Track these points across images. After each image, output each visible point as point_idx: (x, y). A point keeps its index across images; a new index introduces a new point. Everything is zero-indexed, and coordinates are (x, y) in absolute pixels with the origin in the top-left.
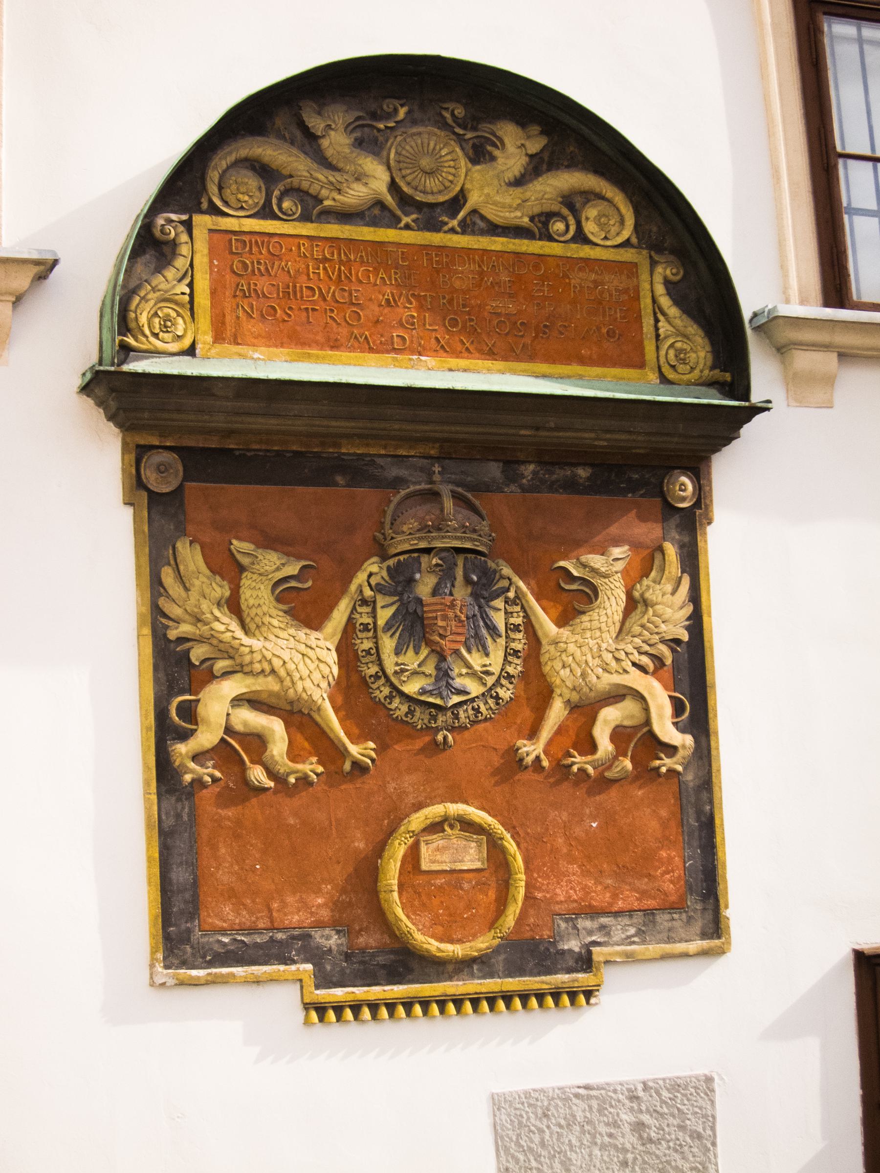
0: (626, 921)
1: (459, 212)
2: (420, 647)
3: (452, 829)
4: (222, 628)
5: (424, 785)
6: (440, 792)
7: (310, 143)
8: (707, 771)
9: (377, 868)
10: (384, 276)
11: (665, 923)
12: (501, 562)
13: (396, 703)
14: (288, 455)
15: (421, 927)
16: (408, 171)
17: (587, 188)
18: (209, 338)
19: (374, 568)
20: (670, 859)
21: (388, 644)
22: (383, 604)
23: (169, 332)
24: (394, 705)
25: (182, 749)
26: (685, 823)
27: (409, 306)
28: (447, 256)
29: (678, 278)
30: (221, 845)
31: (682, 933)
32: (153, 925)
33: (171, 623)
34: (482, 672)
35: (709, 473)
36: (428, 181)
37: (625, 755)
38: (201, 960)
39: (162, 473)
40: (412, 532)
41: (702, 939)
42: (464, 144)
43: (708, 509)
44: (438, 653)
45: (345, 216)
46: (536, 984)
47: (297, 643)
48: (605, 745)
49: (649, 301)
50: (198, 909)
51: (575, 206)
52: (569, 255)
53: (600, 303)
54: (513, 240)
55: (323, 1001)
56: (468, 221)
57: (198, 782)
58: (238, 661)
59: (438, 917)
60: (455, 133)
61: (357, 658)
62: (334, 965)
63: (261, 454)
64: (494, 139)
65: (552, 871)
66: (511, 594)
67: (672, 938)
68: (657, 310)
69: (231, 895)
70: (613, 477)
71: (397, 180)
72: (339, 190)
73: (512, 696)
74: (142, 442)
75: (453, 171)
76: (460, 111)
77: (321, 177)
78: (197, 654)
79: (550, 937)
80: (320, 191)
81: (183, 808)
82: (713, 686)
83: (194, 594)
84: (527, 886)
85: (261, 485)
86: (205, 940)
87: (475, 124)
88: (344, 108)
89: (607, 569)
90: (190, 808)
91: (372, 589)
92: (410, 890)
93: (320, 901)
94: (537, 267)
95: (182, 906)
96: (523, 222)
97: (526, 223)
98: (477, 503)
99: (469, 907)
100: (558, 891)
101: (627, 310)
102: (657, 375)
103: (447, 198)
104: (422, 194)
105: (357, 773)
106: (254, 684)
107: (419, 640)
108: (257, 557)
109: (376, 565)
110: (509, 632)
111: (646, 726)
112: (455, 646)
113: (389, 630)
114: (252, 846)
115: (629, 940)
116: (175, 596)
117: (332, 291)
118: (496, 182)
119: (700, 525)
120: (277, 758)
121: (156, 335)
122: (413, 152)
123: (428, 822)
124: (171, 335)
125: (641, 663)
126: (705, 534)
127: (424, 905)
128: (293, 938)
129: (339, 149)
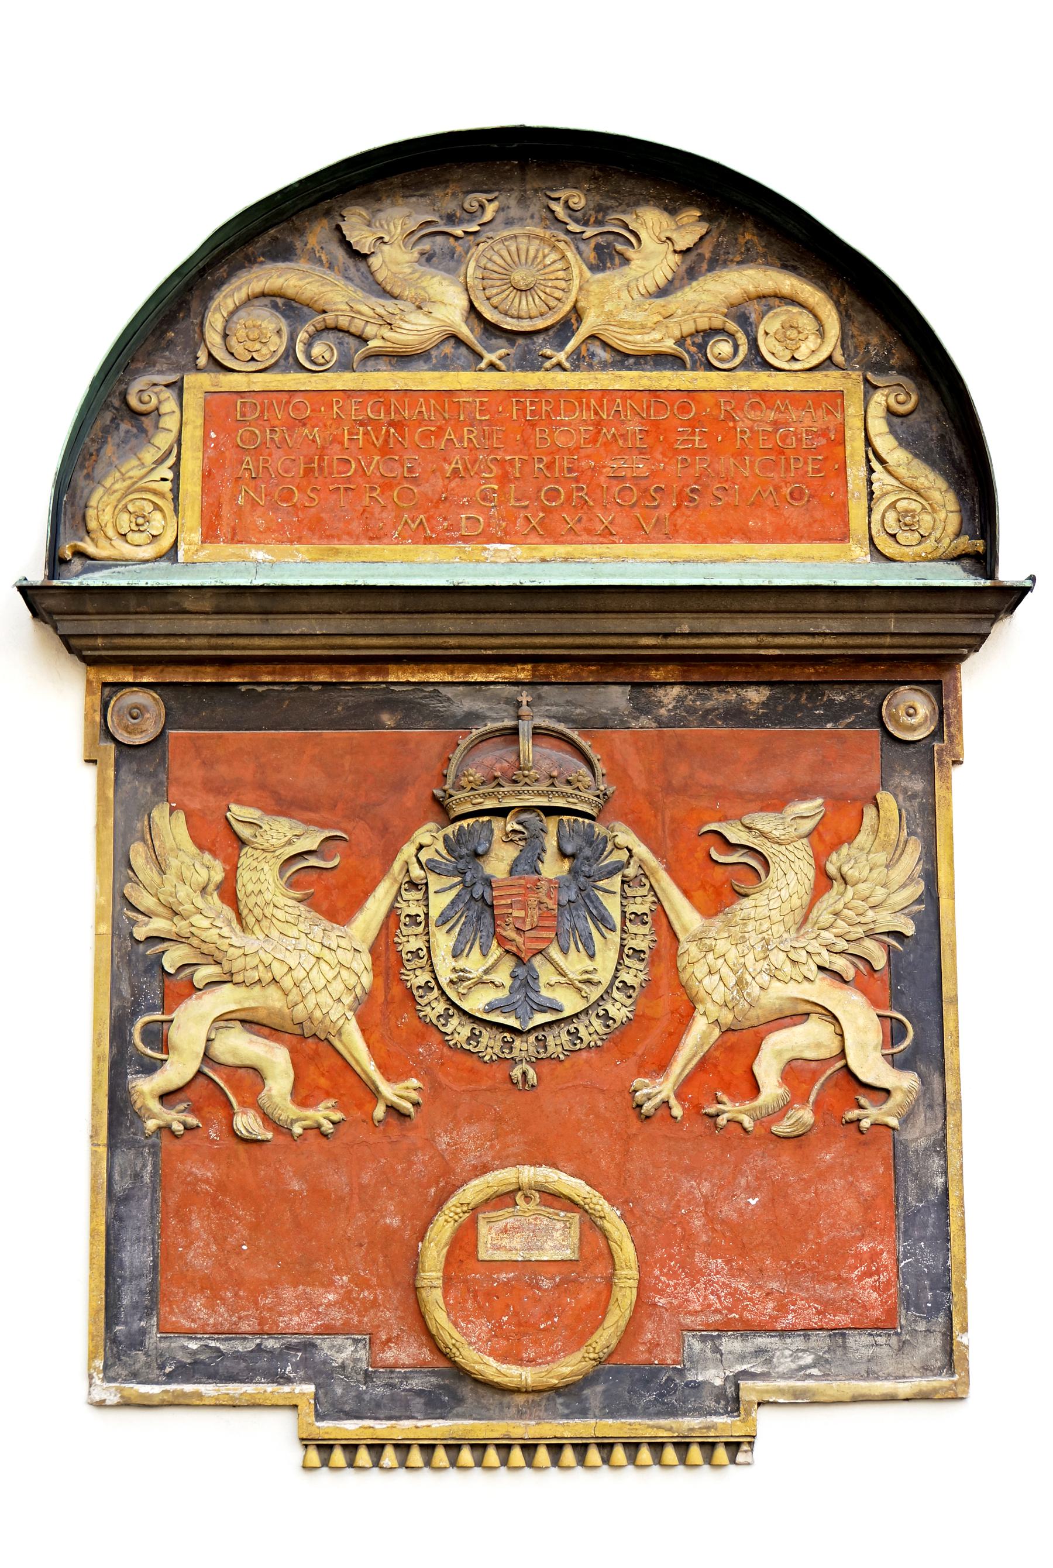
0: (798, 1342)
1: (569, 339)
4: (206, 923)
5: (491, 1140)
6: (512, 1150)
7: (355, 265)
8: (940, 1126)
9: (418, 1255)
11: (863, 1350)
13: (454, 1022)
15: (474, 1340)
16: (494, 291)
17: (766, 291)
18: (197, 537)
19: (426, 839)
20: (875, 1255)
21: (443, 942)
22: (438, 888)
29: (909, 406)
30: (194, 1216)
31: (890, 1367)
32: (93, 1321)
33: (140, 916)
35: (956, 689)
36: (524, 302)
38: (157, 1372)
39: (134, 718)
40: (474, 787)
43: (955, 739)
44: (514, 954)
45: (402, 359)
46: (650, 1430)
49: (860, 443)
50: (157, 1304)
53: (781, 452)
54: (648, 374)
56: (584, 353)
58: (226, 968)
59: (500, 1326)
60: (568, 232)
61: (401, 963)
62: (347, 1388)
65: (683, 1267)
66: (631, 871)
67: (874, 1373)
68: (871, 456)
70: (803, 700)
71: (476, 304)
73: (630, 1015)
74: (110, 679)
75: (563, 284)
76: (576, 200)
77: (364, 309)
79: (675, 1362)
80: (364, 328)
81: (144, 1166)
82: (954, 1000)
83: (171, 877)
85: (276, 729)
86: (163, 1345)
88: (406, 211)
89: (783, 832)
90: (155, 1166)
91: (422, 868)
93: (331, 1297)
94: (684, 408)
95: (136, 1298)
98: (585, 744)
99: (549, 1316)
101: (826, 459)
102: (867, 549)
103: (549, 322)
104: (514, 321)
105: (393, 1121)
106: (247, 999)
107: (488, 936)
109: (428, 834)
110: (628, 923)
111: (841, 1059)
112: (541, 946)
113: (444, 923)
114: (237, 1218)
116: (146, 882)
117: (375, 462)
118: (625, 294)
119: (939, 765)
120: (277, 1100)
122: (502, 263)
123: (491, 1191)
124: (144, 535)
127: (480, 1307)
128: (289, 1347)
129: (394, 269)
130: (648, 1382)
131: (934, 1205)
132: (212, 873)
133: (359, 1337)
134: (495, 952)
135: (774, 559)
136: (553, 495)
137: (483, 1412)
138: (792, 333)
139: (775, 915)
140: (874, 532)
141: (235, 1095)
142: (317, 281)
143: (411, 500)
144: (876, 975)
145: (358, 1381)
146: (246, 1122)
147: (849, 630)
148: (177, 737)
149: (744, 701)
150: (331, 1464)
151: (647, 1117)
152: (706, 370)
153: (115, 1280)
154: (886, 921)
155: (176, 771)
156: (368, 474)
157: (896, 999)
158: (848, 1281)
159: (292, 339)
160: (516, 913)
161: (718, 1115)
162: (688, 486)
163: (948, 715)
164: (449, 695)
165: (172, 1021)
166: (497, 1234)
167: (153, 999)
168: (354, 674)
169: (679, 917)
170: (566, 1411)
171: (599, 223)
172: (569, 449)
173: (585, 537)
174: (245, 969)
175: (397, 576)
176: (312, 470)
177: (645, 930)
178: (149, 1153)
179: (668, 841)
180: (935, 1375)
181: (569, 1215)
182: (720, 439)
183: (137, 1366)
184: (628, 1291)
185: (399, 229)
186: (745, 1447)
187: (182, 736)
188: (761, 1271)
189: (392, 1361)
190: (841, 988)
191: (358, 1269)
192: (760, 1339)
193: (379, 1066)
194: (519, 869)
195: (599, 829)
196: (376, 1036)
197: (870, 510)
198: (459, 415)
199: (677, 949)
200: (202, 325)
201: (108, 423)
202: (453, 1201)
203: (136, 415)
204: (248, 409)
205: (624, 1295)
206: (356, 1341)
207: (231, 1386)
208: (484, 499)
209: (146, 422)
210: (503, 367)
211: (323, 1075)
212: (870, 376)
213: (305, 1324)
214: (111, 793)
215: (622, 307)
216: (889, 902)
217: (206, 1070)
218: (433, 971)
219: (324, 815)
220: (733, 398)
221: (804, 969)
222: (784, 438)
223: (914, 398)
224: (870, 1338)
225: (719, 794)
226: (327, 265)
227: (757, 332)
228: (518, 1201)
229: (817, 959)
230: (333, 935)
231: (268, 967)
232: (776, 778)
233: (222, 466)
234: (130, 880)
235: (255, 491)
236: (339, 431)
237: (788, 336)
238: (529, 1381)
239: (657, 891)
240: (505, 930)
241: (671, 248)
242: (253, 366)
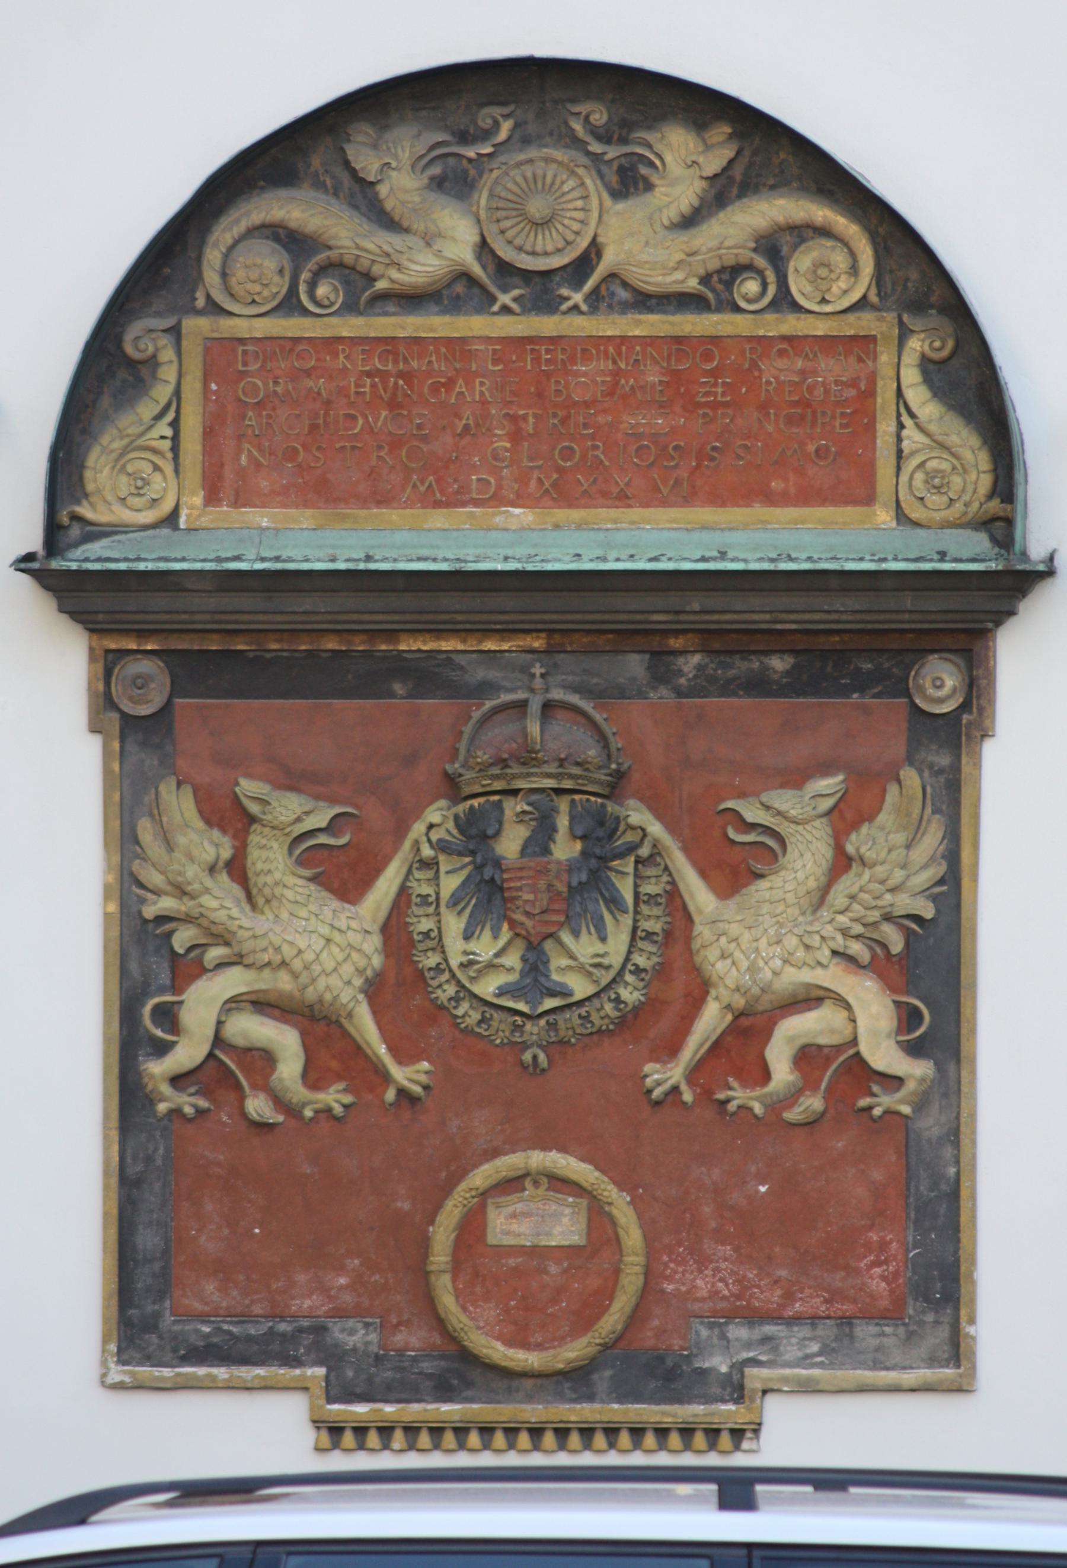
0: (804, 1331)
2: (500, 929)
4: (214, 904)
8: (954, 1115)
10: (464, 390)
12: (632, 802)
13: (464, 1007)
14: (324, 655)
15: (482, 1324)
18: (198, 500)
20: (884, 1245)
22: (449, 868)
24: (460, 1012)
26: (912, 1190)
28: (564, 350)
29: (945, 353)
31: (896, 1357)
32: (106, 1307)
33: (149, 895)
36: (540, 237)
38: (171, 1355)
39: (139, 688)
42: (605, 169)
44: (524, 938)
47: (320, 923)
49: (891, 395)
52: (761, 333)
54: (671, 318)
57: (176, 1113)
58: (236, 949)
60: (588, 153)
61: (412, 944)
63: (285, 654)
66: (644, 851)
67: (881, 1363)
68: (903, 410)
70: (829, 669)
71: (489, 240)
77: (371, 246)
78: (183, 938)
79: (683, 1349)
81: (156, 1149)
89: (800, 811)
93: (343, 1281)
95: (149, 1281)
96: (688, 287)
97: (694, 288)
98: (598, 717)
101: (855, 412)
102: (893, 513)
108: (269, 803)
109: (439, 813)
112: (552, 930)
113: (455, 904)
115: (808, 1361)
120: (288, 1083)
125: (850, 952)
128: (301, 1330)
132: (221, 851)
133: (371, 1320)
134: (506, 934)
136: (567, 453)
138: (823, 272)
139: (790, 898)
141: (246, 1077)
142: (321, 213)
144: (894, 959)
146: (257, 1106)
147: (864, 608)
151: (658, 1103)
154: (904, 903)
156: (376, 430)
157: (911, 985)
158: (857, 1271)
164: (463, 663)
165: (181, 1003)
166: (506, 1218)
168: (363, 642)
170: (574, 1396)
172: (585, 402)
176: (317, 426)
177: (657, 911)
178: (162, 1136)
181: (578, 1200)
182: (744, 390)
183: (151, 1349)
185: (408, 152)
186: (749, 1435)
190: (856, 974)
193: (391, 1049)
195: (611, 807)
197: (899, 468)
202: (463, 1186)
206: (367, 1325)
207: (243, 1369)
208: (495, 458)
213: (317, 1308)
214: (116, 767)
216: (909, 884)
217: (218, 1052)
218: (443, 952)
222: (811, 389)
223: (950, 344)
229: (833, 945)
230: (343, 917)
231: (277, 949)
237: (820, 272)
238: (536, 1364)
239: (672, 870)
241: (698, 173)
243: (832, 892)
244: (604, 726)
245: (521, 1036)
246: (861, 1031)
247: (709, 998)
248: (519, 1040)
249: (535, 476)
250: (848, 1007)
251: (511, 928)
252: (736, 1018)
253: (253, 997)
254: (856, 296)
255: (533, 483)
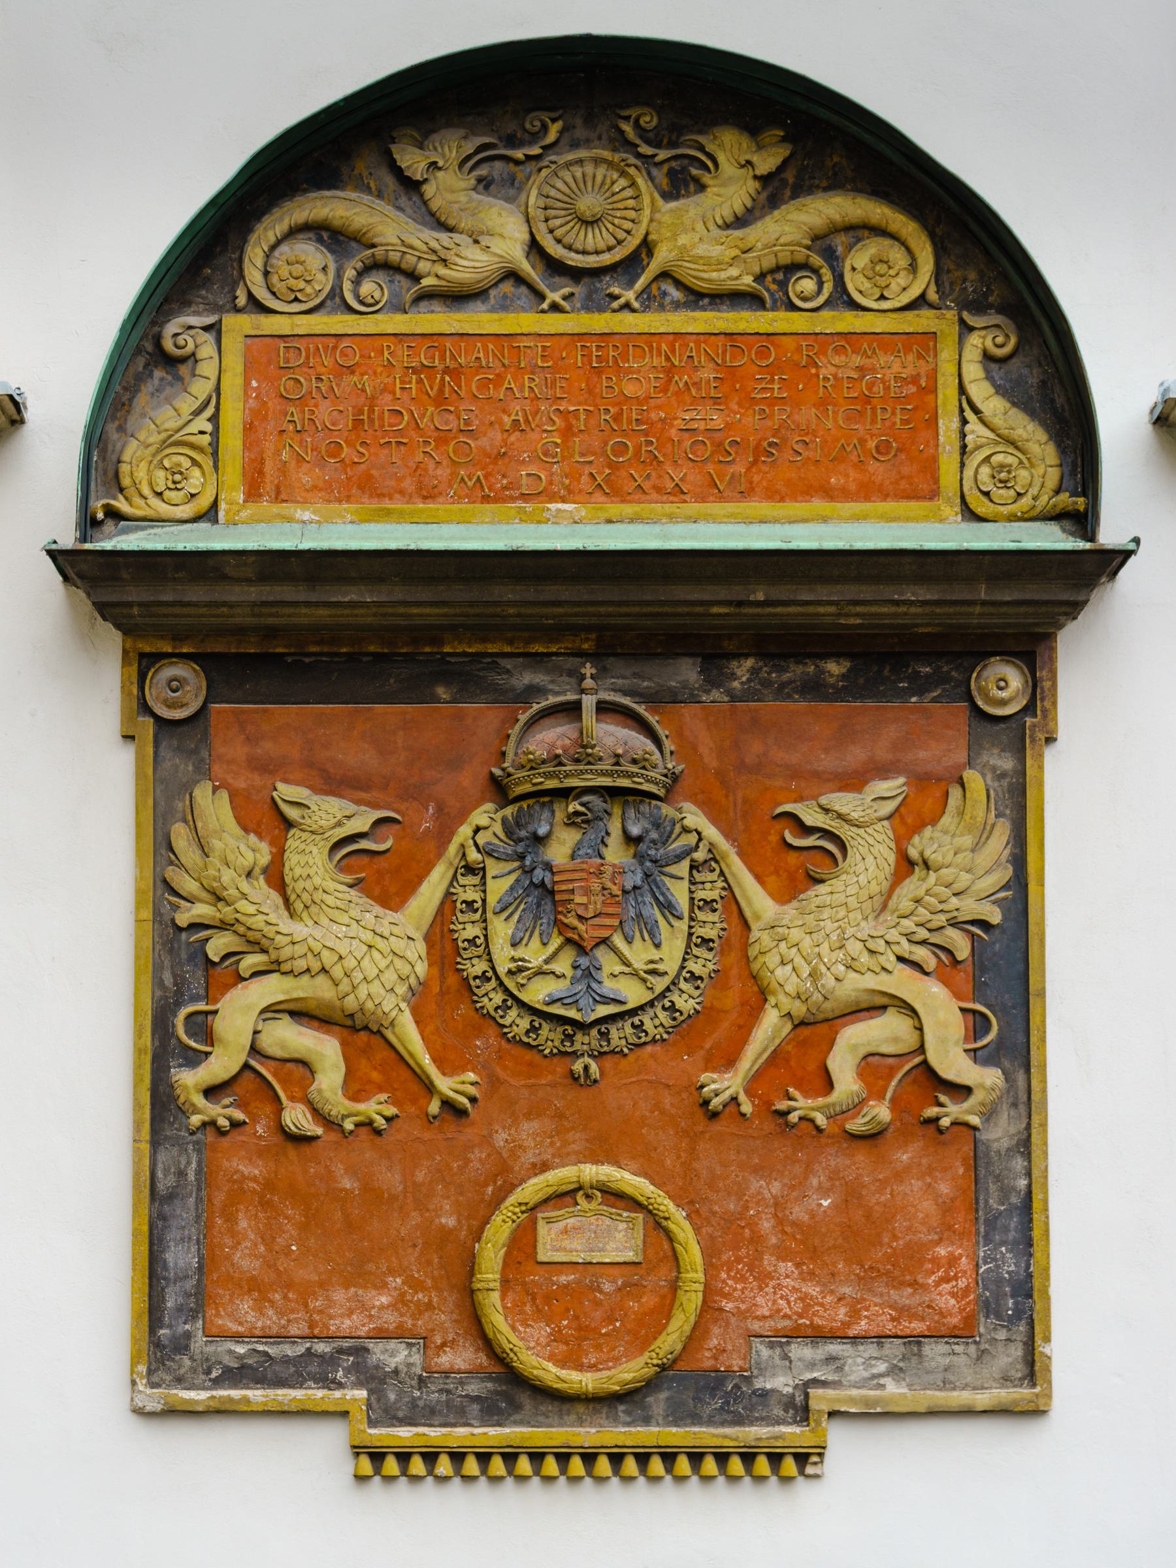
0: (870, 1350)
1: (638, 276)
3: (589, 1203)
4: (251, 909)
5: (551, 1137)
7: (406, 193)
8: (1024, 1125)
9: (474, 1256)
10: (513, 386)
11: (939, 1359)
12: (688, 806)
13: (513, 1014)
15: (532, 1344)
17: (854, 221)
19: (483, 821)
20: (953, 1261)
21: (502, 930)
23: (179, 490)
24: (507, 1021)
25: (189, 1080)
26: (982, 1204)
27: (549, 428)
30: (241, 1215)
32: (136, 1324)
33: (182, 902)
34: (645, 972)
35: (1052, 660)
36: (590, 235)
37: (881, 1096)
38: (203, 1377)
41: (1002, 1387)
43: (1049, 715)
46: (715, 1439)
48: (847, 1083)
50: (203, 1306)
51: (835, 251)
53: (867, 400)
54: (725, 315)
55: (379, 1444)
56: (655, 291)
58: (274, 957)
59: (560, 1331)
62: (401, 1394)
64: (703, 158)
65: (751, 1270)
68: (965, 405)
69: (254, 1287)
70: (886, 673)
71: (538, 238)
72: (445, 261)
73: (698, 1007)
75: (632, 214)
76: (648, 119)
77: (417, 243)
79: (742, 1369)
81: (189, 1163)
82: (1042, 994)
83: (214, 860)
84: (709, 1291)
86: (210, 1349)
87: (674, 137)
88: (462, 132)
89: (862, 814)
91: (479, 851)
92: (519, 1288)
93: (384, 1300)
94: (763, 352)
95: (180, 1300)
96: (743, 284)
97: (748, 285)
98: (652, 719)
99: (610, 1319)
100: (760, 1300)
101: (915, 409)
102: (958, 509)
103: (618, 258)
104: (580, 257)
105: (448, 1117)
107: (549, 924)
108: (309, 808)
109: (486, 815)
110: (696, 911)
112: (605, 933)
113: (503, 910)
114: (286, 1217)
115: (875, 1382)
116: (189, 865)
118: (700, 226)
121: (160, 494)
122: (567, 191)
123: (550, 1190)
124: (182, 493)
125: (914, 958)
126: (1041, 756)
127: (539, 1311)
128: (340, 1351)
129: (449, 197)
130: (713, 1389)
131: (1017, 1208)
132: (258, 855)
135: (857, 518)
136: (621, 448)
137: (541, 1419)
140: (966, 489)
141: (285, 1090)
143: (468, 455)
145: (412, 1387)
146: (296, 1117)
148: (219, 712)
149: (823, 672)
150: (385, 1472)
151: (715, 1115)
152: (786, 310)
153: (158, 1281)
154: (970, 908)
155: (220, 748)
157: (979, 992)
158: (924, 1287)
159: (339, 276)
160: (579, 899)
161: (789, 1112)
162: (766, 439)
163: (1042, 688)
165: (216, 1012)
167: (196, 988)
169: (750, 903)
171: (673, 145)
173: (654, 496)
174: (292, 958)
175: (453, 538)
177: (714, 917)
178: (194, 1150)
179: (740, 823)
180: (1015, 1386)
181: (633, 1215)
182: (801, 387)
183: (182, 1371)
184: (693, 1294)
186: (815, 1459)
187: (224, 711)
188: (833, 1275)
189: (447, 1366)
191: (412, 1270)
192: (831, 1347)
193: (434, 1060)
194: (581, 853)
195: (666, 810)
196: (430, 1028)
197: (963, 465)
198: (519, 362)
199: (748, 938)
200: (240, 260)
201: (141, 369)
202: (512, 1199)
203: (172, 362)
204: (292, 354)
205: (689, 1300)
206: (410, 1345)
207: (280, 1392)
208: (545, 455)
209: (184, 370)
210: (568, 308)
211: (375, 1068)
212: (966, 315)
214: (150, 771)
215: (697, 240)
216: (974, 888)
217: (253, 1063)
218: (490, 960)
219: (375, 795)
220: (815, 341)
221: (882, 959)
222: (870, 386)
223: (1013, 341)
224: (947, 1347)
225: (795, 773)
226: (376, 193)
227: (843, 267)
228: (579, 1201)
230: (386, 922)
231: (317, 955)
232: (856, 755)
233: (265, 418)
234: (171, 863)
235: (301, 446)
236: (390, 380)
239: (728, 876)
240: (565, 916)
241: (751, 173)
242: (296, 307)
243: (895, 897)
244: (658, 727)
245: (572, 1044)
246: (929, 1037)
247: (767, 1006)
248: (570, 1050)
249: (586, 472)
250: (913, 1012)
251: (560, 933)
252: (796, 1027)
253: (291, 1006)
254: (914, 292)
255: (585, 479)
